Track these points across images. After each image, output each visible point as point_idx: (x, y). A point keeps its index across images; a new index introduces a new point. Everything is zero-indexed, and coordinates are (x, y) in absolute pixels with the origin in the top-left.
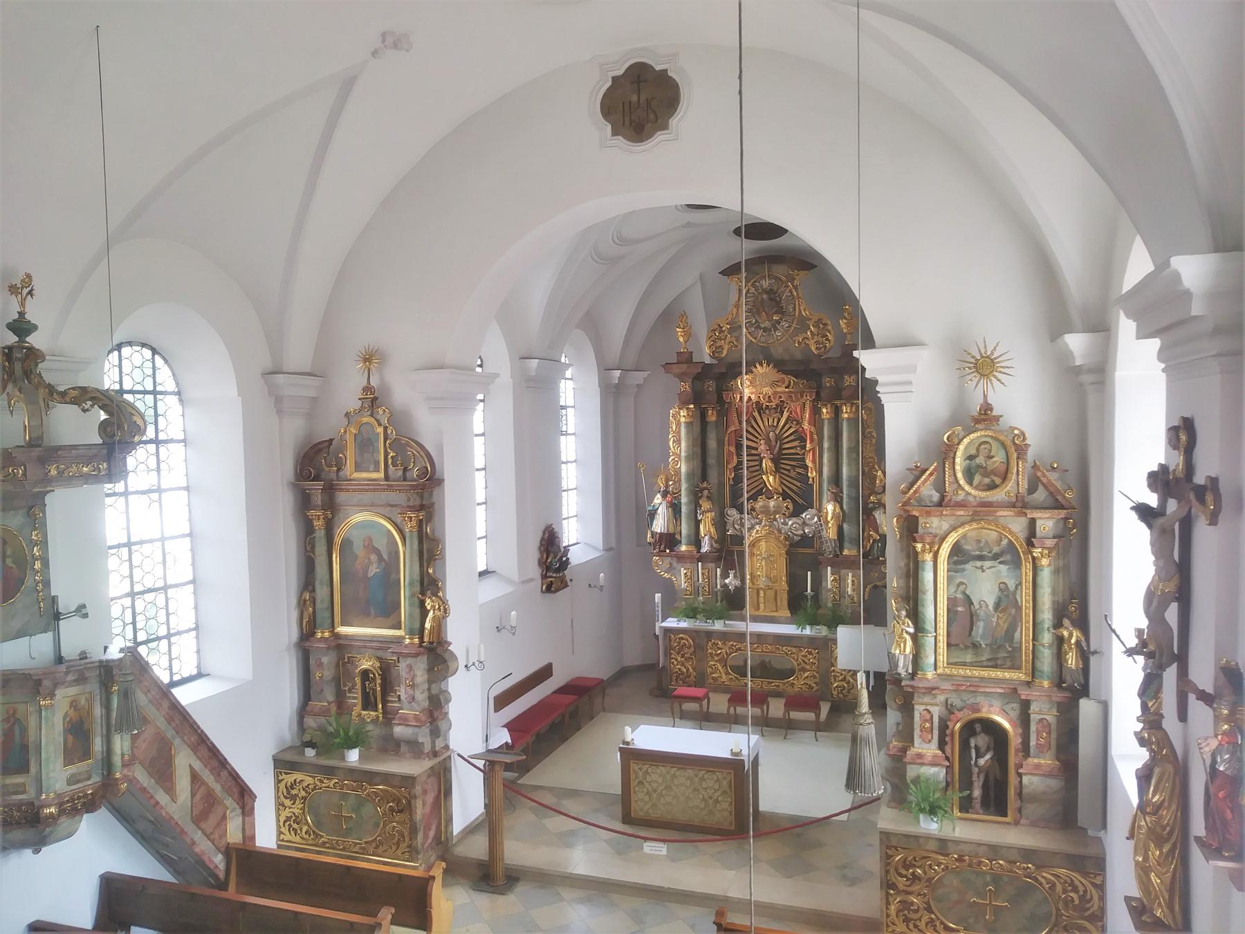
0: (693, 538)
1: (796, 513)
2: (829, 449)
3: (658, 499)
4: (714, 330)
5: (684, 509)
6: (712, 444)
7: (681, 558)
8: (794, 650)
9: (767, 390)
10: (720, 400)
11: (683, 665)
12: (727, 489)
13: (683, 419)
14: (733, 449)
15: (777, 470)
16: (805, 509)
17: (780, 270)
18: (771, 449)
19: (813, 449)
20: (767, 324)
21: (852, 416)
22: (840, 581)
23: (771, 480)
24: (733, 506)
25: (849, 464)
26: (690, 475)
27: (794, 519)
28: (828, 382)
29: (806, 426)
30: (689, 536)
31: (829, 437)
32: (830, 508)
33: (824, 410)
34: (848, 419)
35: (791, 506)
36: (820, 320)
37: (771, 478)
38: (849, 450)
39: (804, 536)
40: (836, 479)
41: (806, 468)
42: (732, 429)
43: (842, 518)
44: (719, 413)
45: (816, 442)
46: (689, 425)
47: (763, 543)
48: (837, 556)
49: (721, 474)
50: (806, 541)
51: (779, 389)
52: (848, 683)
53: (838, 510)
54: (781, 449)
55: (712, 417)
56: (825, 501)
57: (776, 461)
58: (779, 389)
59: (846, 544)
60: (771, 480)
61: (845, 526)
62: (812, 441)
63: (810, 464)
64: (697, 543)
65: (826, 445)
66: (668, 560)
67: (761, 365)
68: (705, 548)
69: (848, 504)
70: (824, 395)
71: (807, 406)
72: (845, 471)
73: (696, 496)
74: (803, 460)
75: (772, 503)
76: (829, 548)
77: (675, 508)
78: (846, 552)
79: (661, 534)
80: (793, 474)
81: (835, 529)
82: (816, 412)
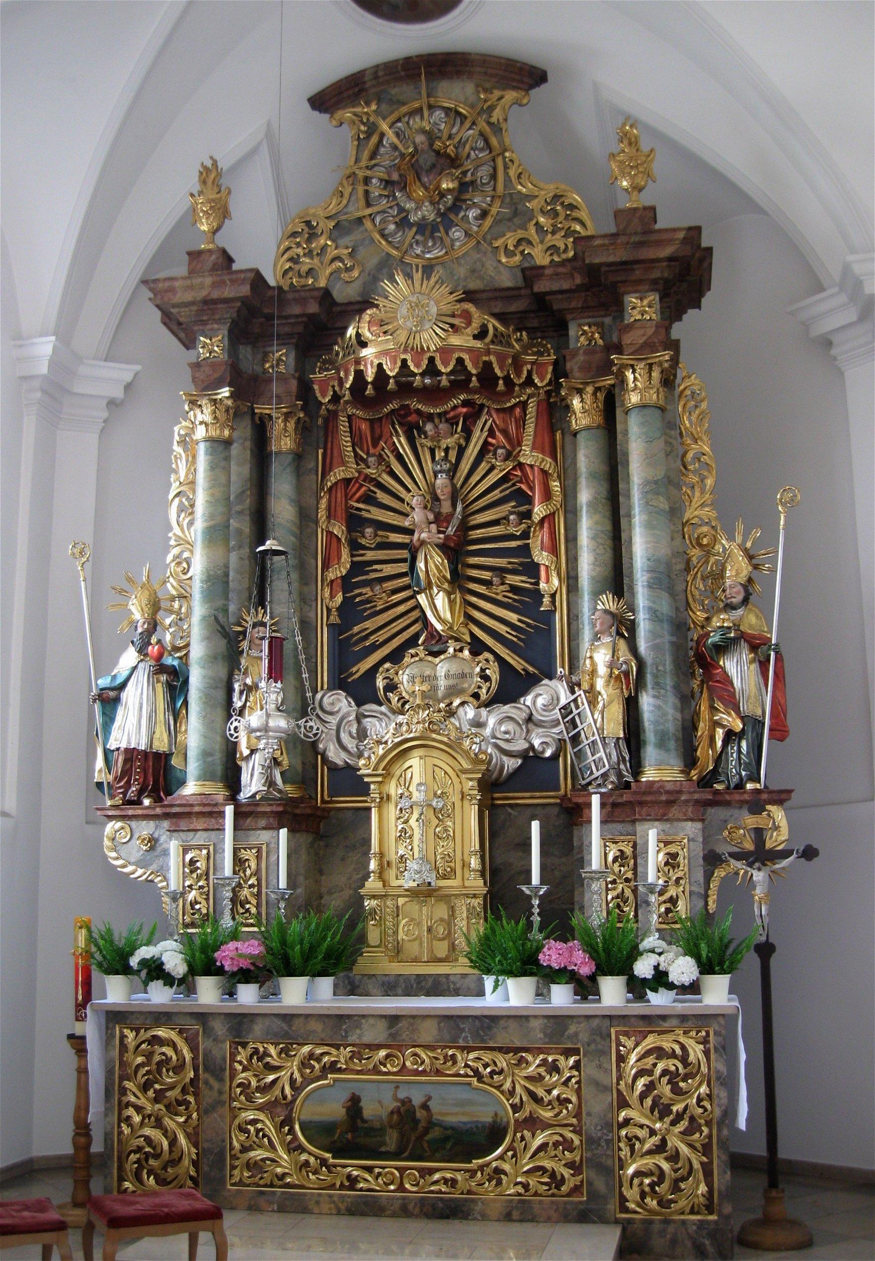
0: (218, 757)
1: (511, 688)
2: (591, 505)
3: (130, 657)
4: (294, 234)
5: (196, 678)
6: (282, 508)
7: (180, 818)
8: (502, 1062)
9: (431, 338)
10: (305, 390)
11: (158, 1124)
12: (324, 636)
13: (201, 432)
14: (339, 529)
15: (457, 581)
16: (528, 682)
17: (456, 93)
18: (440, 520)
19: (550, 518)
20: (427, 212)
21: (653, 397)
22: (633, 859)
23: (439, 607)
24: (340, 682)
25: (649, 526)
26: (218, 583)
27: (507, 709)
28: (582, 335)
29: (529, 456)
30: (205, 754)
31: (592, 476)
32: (600, 657)
33: (576, 403)
34: (642, 406)
35: (494, 672)
36: (556, 197)
37: (441, 600)
38: (653, 487)
39: (530, 757)
40: (617, 580)
41: (532, 570)
42: (338, 474)
43: (632, 684)
44: (304, 430)
45: (558, 497)
46: (220, 446)
47: (415, 764)
48: (627, 785)
49: (305, 600)
50: (534, 769)
51: (455, 340)
52: (674, 1157)
53: (624, 653)
54: (465, 527)
55: (283, 440)
56: (586, 635)
57: (454, 551)
58: (455, 340)
59: (650, 753)
60: (439, 607)
61: (646, 702)
62: (547, 496)
63: (542, 557)
64: (231, 778)
65: (584, 496)
66: (145, 828)
67: (409, 276)
68: (252, 783)
69: (653, 635)
70: (571, 365)
71: (532, 408)
72: (641, 547)
73: (230, 647)
74: (525, 550)
75: (443, 668)
76: (601, 760)
77: (174, 682)
78: (649, 775)
79: (130, 754)
80: (500, 591)
81: (616, 712)
82: (555, 412)
